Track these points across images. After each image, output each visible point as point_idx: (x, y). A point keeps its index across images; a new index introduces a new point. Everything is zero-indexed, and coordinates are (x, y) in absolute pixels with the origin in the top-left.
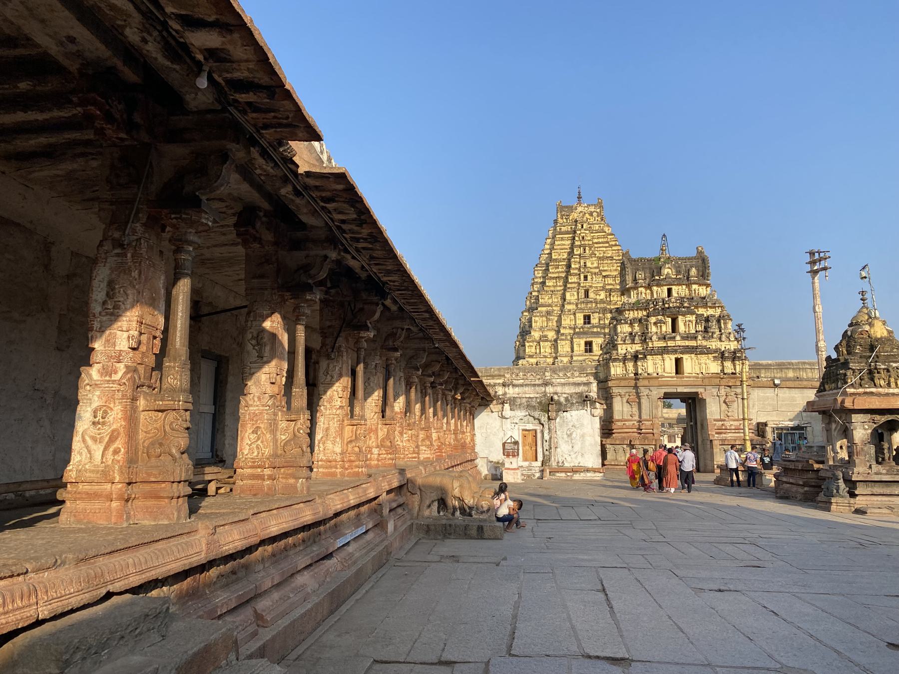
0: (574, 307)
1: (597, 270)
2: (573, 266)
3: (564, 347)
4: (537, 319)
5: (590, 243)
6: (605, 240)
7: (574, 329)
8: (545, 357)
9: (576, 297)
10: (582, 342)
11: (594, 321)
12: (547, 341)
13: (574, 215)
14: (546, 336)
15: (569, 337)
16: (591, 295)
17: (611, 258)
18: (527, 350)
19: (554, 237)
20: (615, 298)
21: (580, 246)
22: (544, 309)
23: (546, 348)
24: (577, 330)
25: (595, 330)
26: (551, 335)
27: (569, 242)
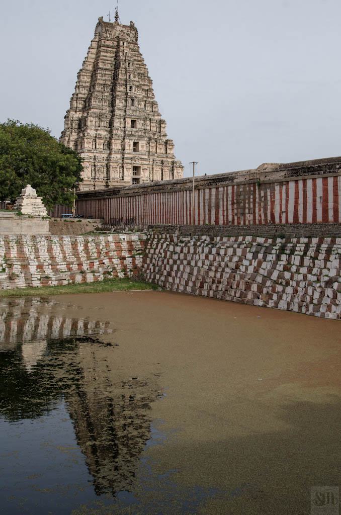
3: (116, 145)
4: (92, 119)
10: (132, 143)
11: (139, 125)
24: (127, 132)
25: (140, 134)
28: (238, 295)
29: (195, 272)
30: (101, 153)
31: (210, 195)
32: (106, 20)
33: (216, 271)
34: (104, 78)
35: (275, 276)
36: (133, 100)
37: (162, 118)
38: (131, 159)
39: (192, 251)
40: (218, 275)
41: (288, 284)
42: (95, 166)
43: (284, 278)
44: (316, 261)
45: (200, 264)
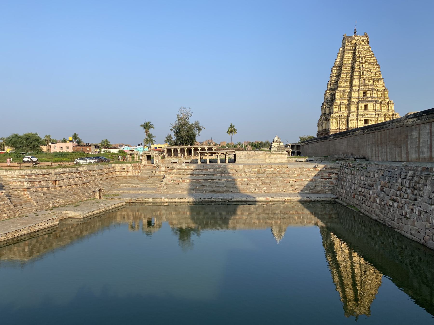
0: (357, 88)
1: (368, 69)
2: (356, 67)
3: (353, 108)
4: (338, 94)
5: (364, 55)
6: (370, 54)
7: (359, 99)
8: (343, 113)
9: (358, 83)
11: (368, 94)
12: (344, 105)
13: (354, 41)
14: (343, 103)
15: (356, 103)
16: (366, 82)
17: (373, 63)
18: (334, 110)
19: (343, 52)
20: (376, 84)
21: (360, 57)
22: (341, 89)
23: (343, 108)
25: (369, 99)
26: (346, 102)
27: (352, 55)
29: (353, 188)
30: (343, 113)
34: (346, 70)
36: (364, 80)
38: (363, 115)
39: (355, 173)
41: (394, 201)
45: (356, 182)
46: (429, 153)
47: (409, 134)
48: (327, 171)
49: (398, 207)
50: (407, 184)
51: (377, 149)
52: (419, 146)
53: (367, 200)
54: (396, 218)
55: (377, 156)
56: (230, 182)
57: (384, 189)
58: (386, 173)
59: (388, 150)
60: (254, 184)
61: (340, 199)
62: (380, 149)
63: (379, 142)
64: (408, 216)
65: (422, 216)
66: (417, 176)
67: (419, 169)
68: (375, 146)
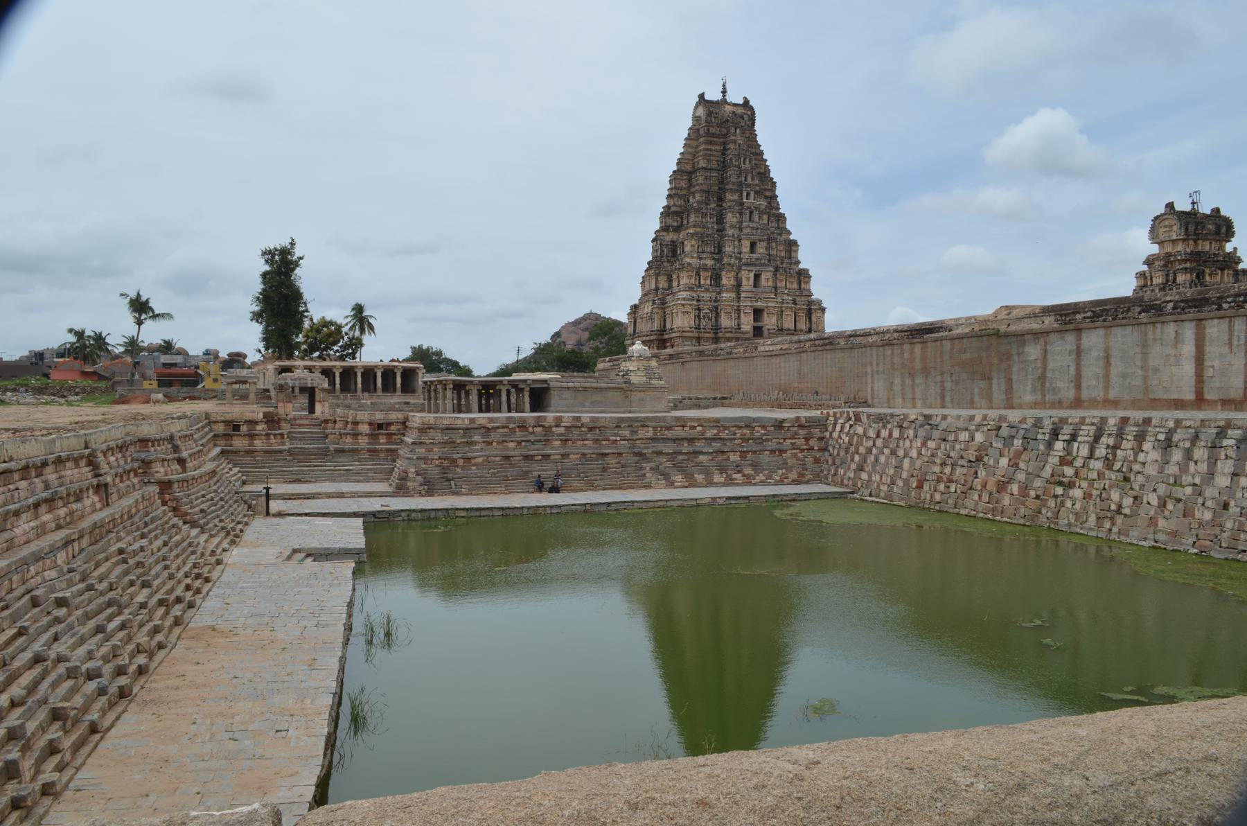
3: (727, 280)
10: (752, 275)
11: (761, 248)
28: (985, 498)
30: (707, 291)
31: (912, 353)
32: (707, 97)
33: (943, 464)
35: (1048, 471)
36: (751, 213)
37: (792, 237)
39: (896, 434)
40: (948, 470)
41: (1071, 485)
42: (699, 309)
43: (1064, 476)
44: (1119, 452)
45: (914, 453)
46: (1071, 394)
47: (1014, 351)
48: (802, 432)
49: (1087, 496)
50: (1085, 451)
51: (908, 381)
52: (1043, 378)
53: (971, 488)
54: (1092, 520)
55: (909, 396)
56: (591, 459)
57: (1022, 465)
58: (1005, 431)
59: (948, 385)
60: (652, 464)
61: (867, 492)
62: (919, 380)
63: (918, 366)
64: (1127, 511)
65: (1170, 506)
66: (1109, 435)
67: (1111, 422)
68: (902, 374)
